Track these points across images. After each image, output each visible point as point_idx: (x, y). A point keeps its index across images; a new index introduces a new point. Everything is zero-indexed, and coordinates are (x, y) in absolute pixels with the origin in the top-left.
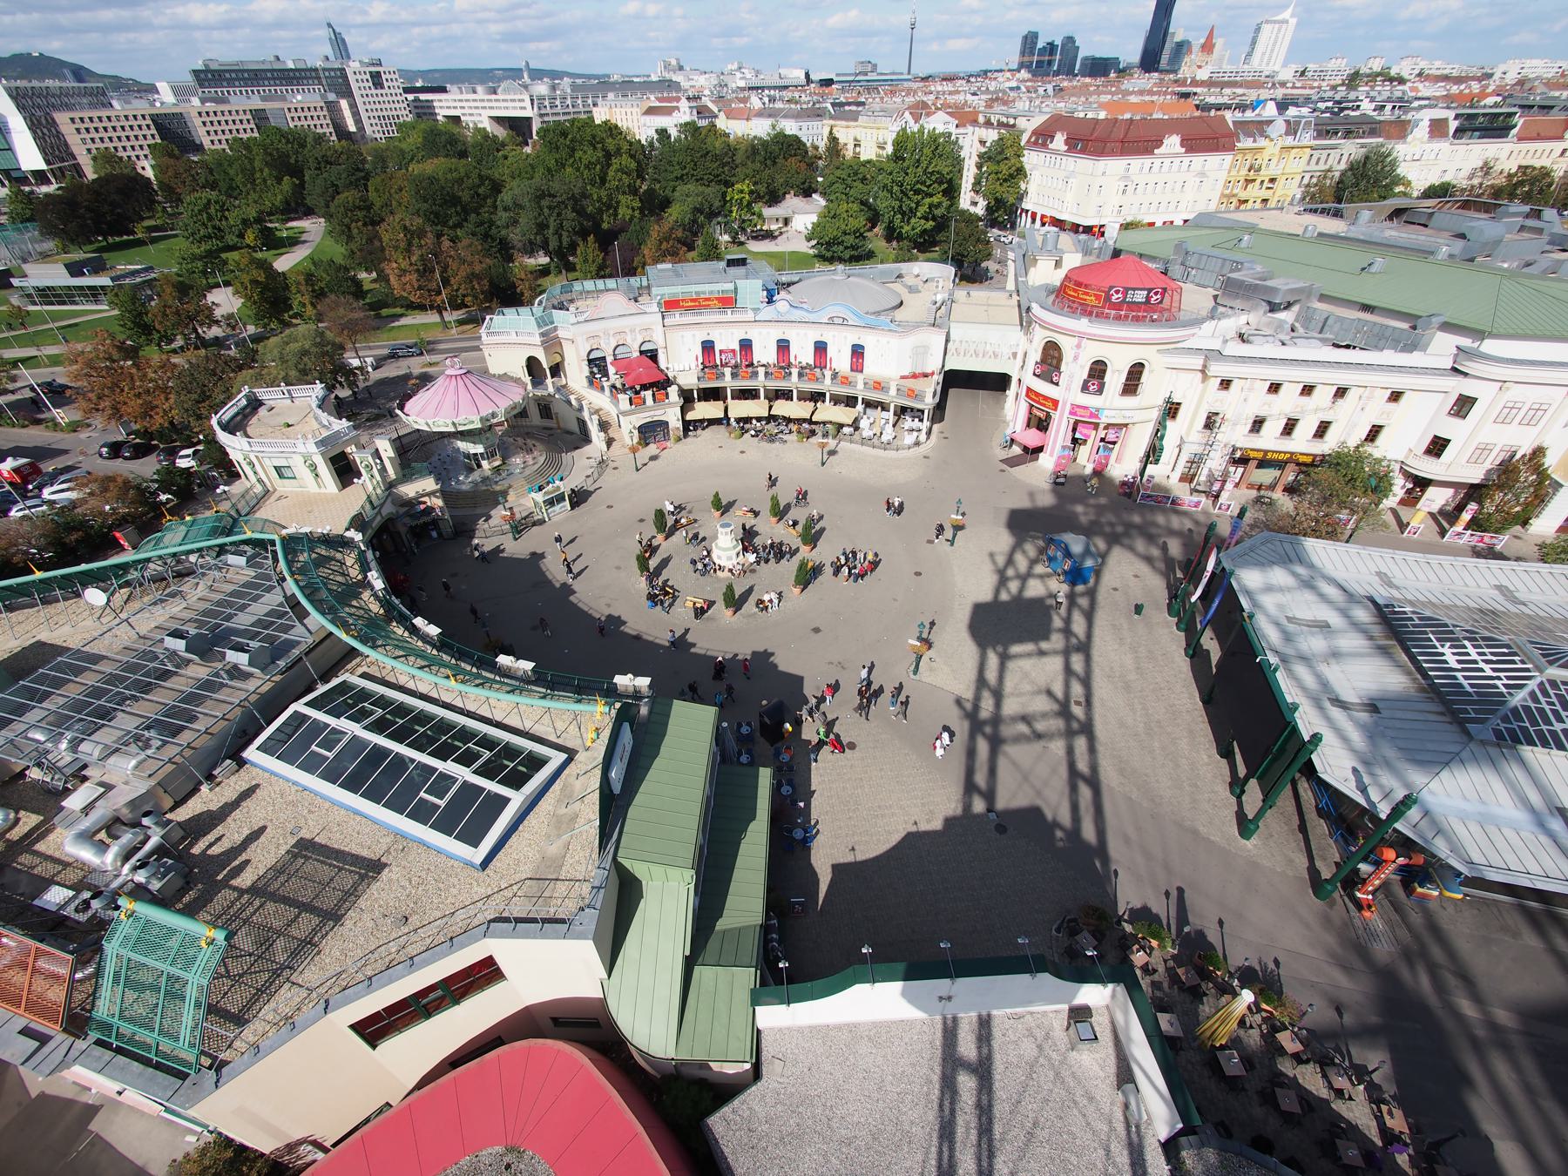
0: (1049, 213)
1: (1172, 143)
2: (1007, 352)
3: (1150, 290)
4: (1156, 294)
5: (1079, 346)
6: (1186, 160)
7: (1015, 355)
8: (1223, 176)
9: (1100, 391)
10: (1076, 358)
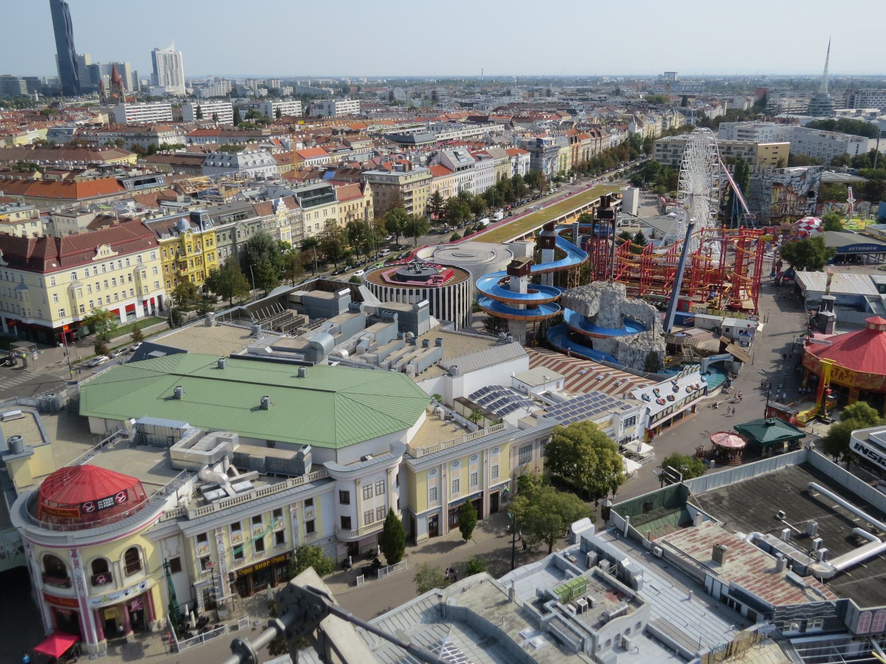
0: (14, 317)
1: (105, 250)
2: (10, 549)
3: (114, 496)
4: (120, 496)
5: (74, 555)
6: (124, 260)
7: (22, 549)
8: (158, 263)
9: (109, 579)
10: (77, 564)
